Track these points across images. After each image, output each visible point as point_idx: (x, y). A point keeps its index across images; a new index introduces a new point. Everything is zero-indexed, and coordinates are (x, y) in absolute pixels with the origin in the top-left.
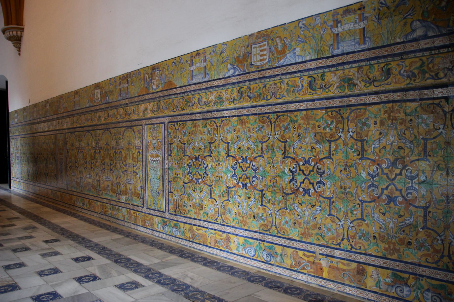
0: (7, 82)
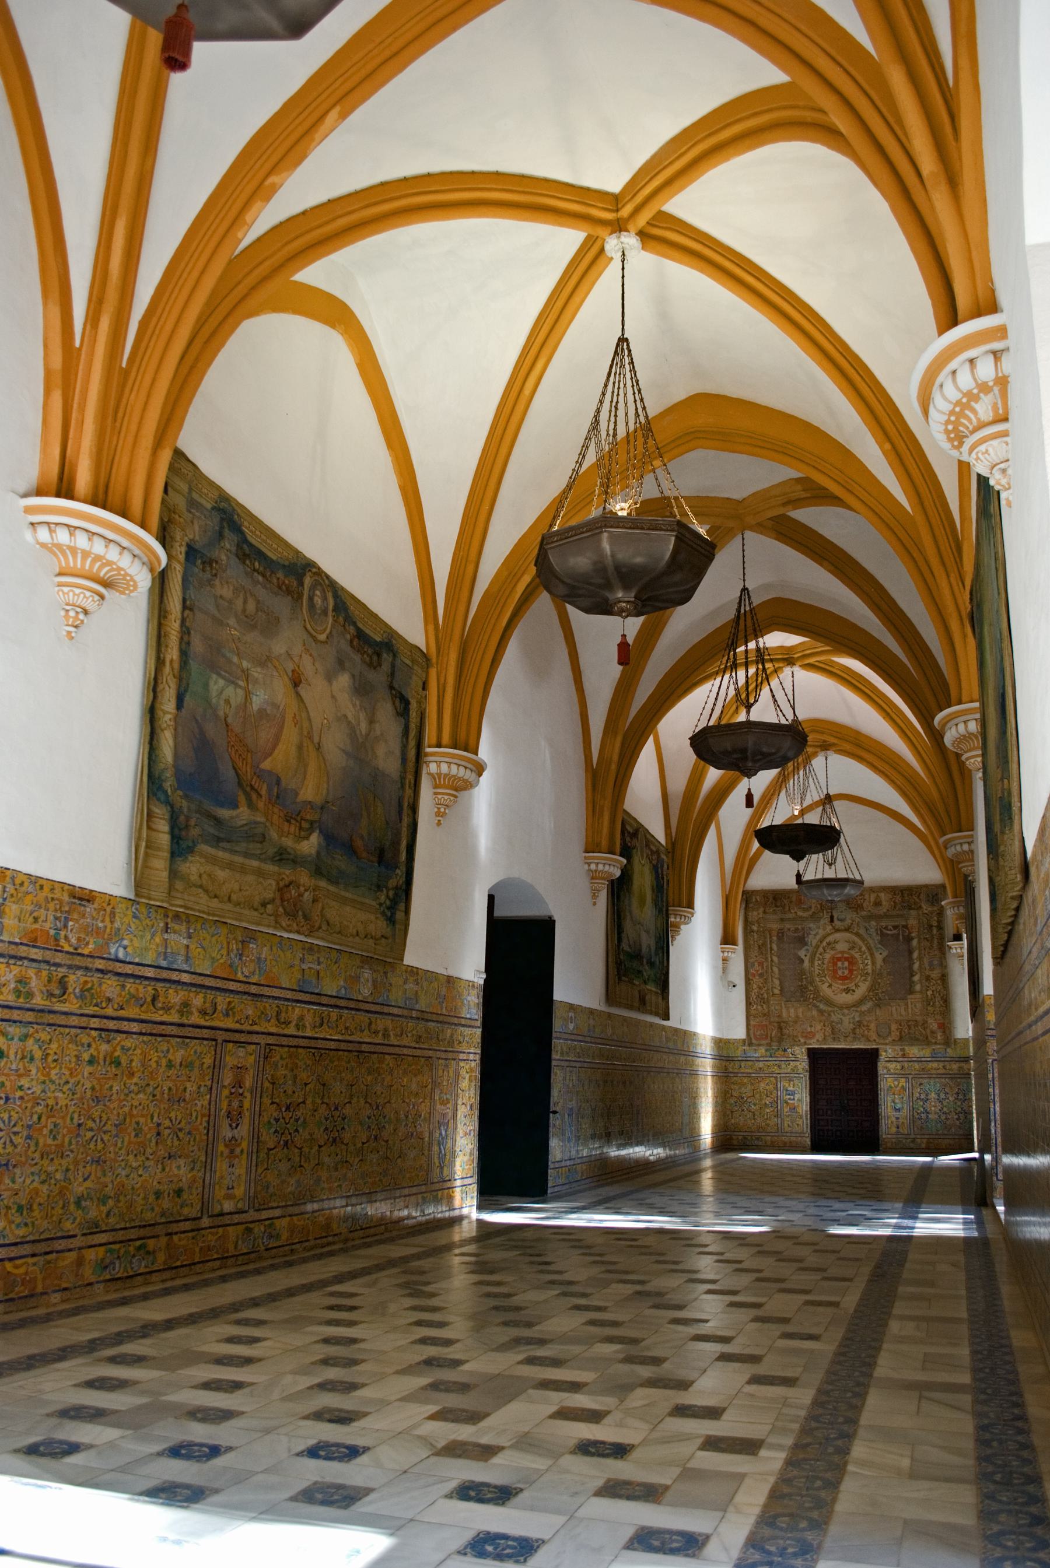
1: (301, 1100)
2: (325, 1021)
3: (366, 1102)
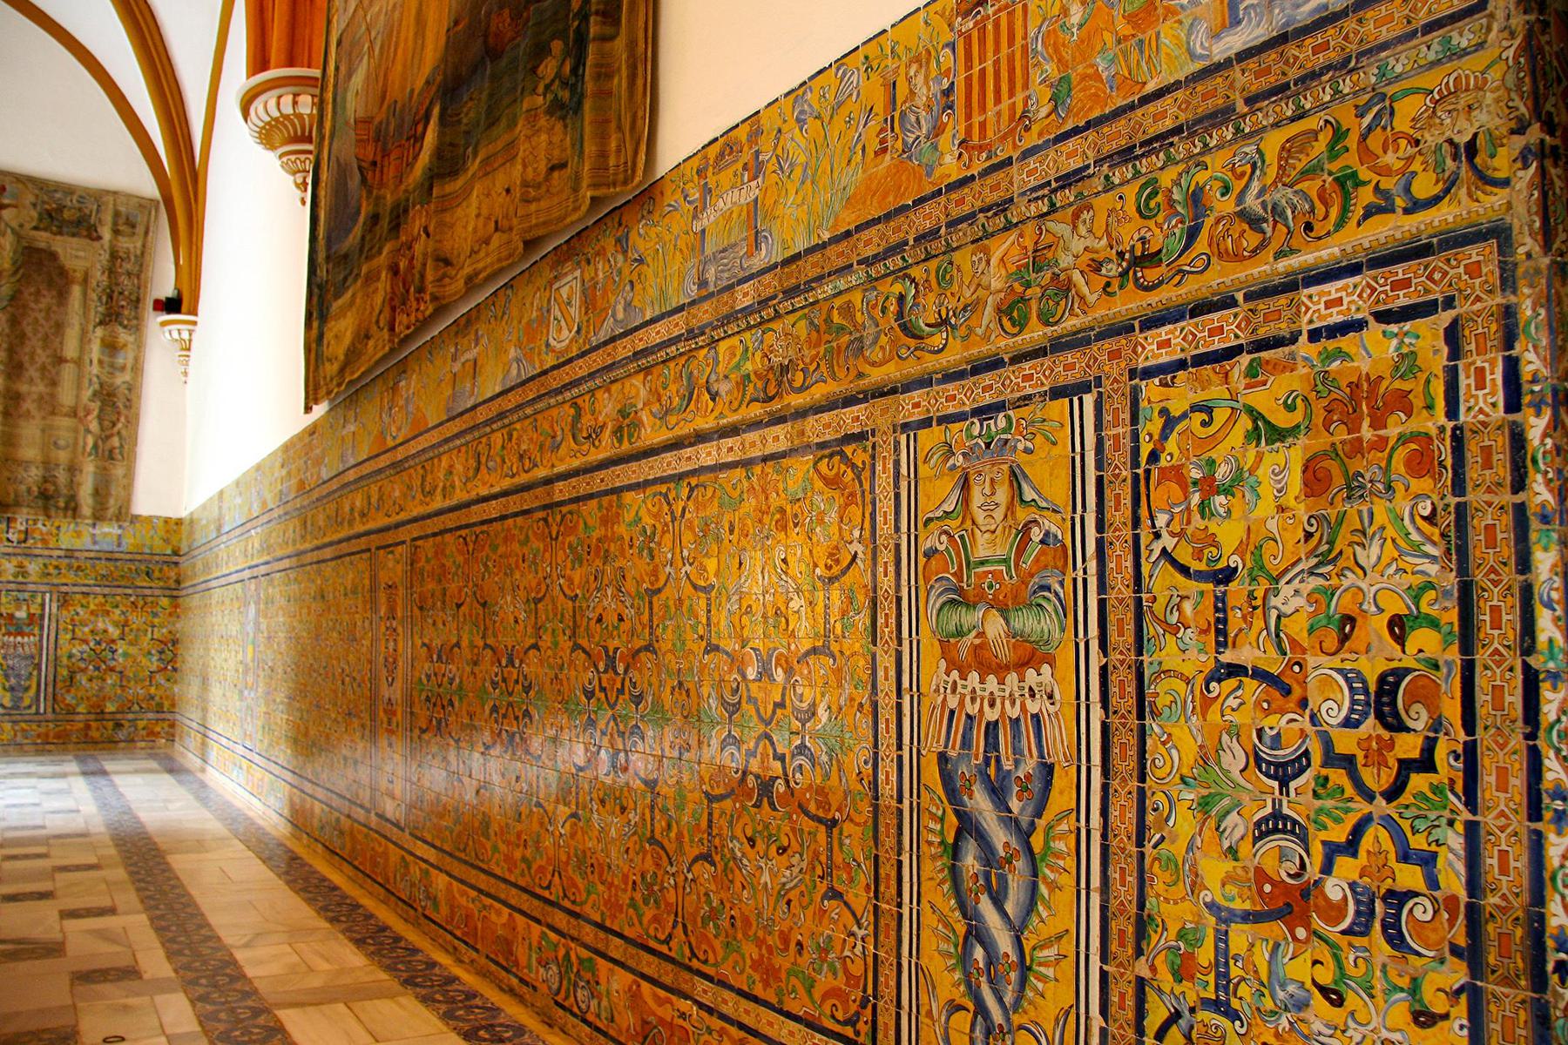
1: (454, 640)
2: (483, 460)
3: (577, 647)
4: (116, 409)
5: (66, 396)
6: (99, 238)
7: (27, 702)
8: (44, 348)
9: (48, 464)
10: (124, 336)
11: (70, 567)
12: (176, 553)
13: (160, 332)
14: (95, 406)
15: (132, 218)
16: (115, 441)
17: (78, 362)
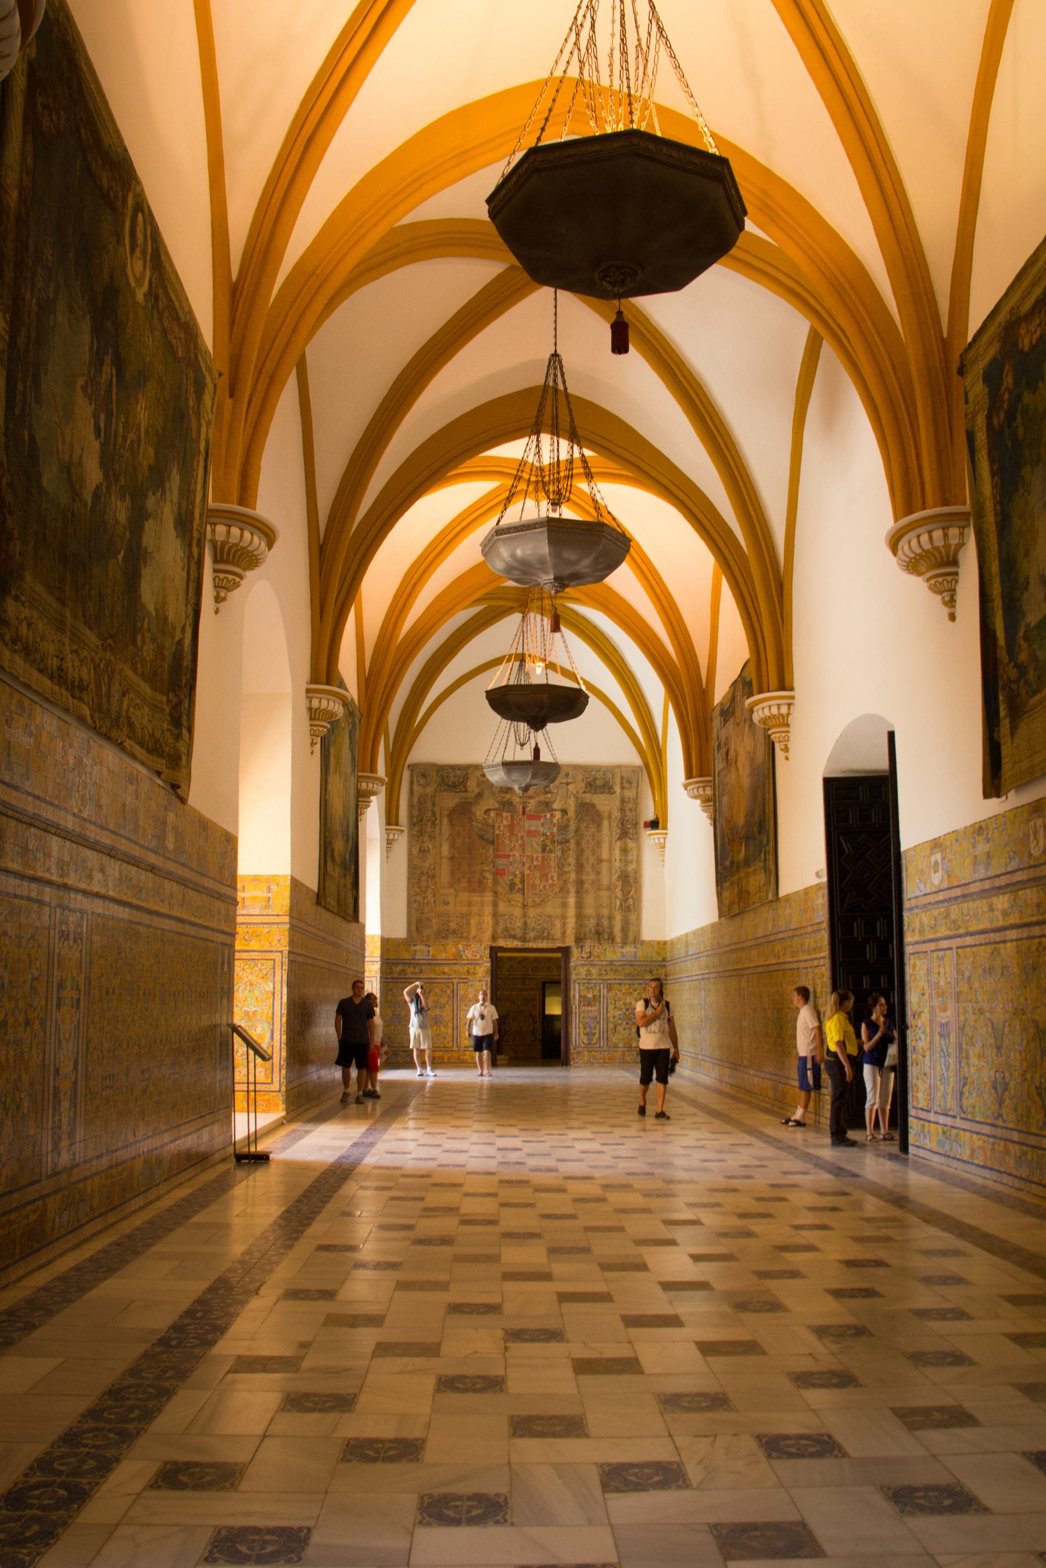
0: (891, 736)
4: (630, 883)
5: (605, 880)
6: (615, 792)
7: (595, 1041)
8: (593, 855)
9: (599, 917)
10: (631, 844)
11: (611, 970)
12: (664, 960)
13: (649, 839)
14: (619, 884)
15: (628, 778)
16: (630, 901)
17: (609, 861)
